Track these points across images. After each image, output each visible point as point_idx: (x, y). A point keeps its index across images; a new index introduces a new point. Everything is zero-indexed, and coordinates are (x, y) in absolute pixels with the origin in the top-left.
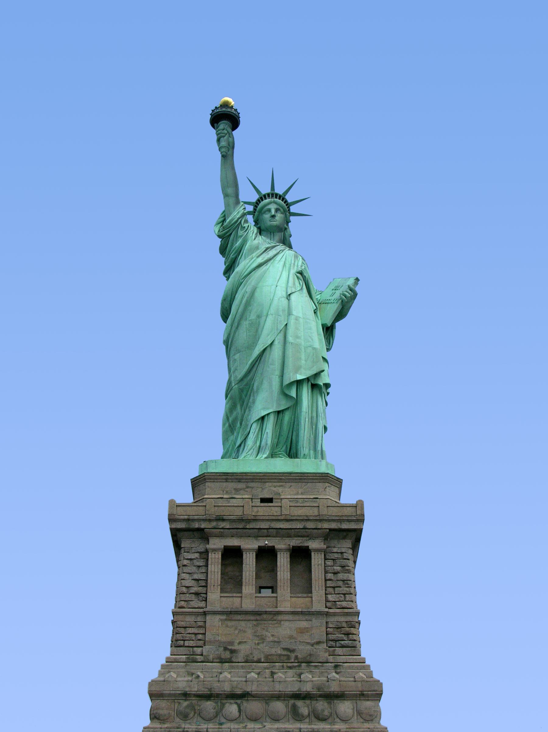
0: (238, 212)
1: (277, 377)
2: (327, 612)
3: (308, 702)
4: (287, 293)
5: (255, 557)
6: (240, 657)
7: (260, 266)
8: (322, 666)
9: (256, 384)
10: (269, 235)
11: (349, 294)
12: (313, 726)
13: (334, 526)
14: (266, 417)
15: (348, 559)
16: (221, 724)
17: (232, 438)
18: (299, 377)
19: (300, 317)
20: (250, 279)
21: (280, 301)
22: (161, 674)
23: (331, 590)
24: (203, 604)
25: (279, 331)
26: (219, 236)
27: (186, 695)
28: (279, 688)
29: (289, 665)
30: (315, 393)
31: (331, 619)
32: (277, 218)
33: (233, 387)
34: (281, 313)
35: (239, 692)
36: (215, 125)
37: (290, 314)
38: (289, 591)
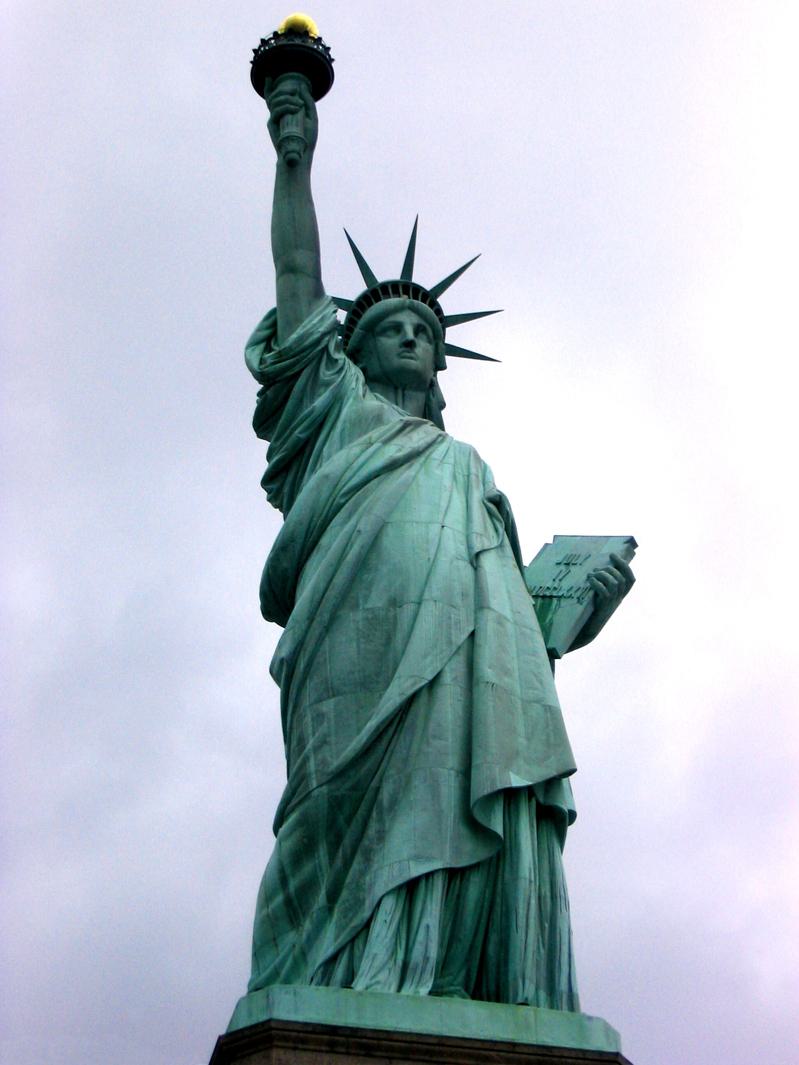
0: (322, 319)
1: (452, 772)
4: (469, 547)
7: (393, 466)
10: (392, 395)
11: (616, 578)
14: (423, 884)
17: (291, 938)
18: (517, 781)
19: (505, 618)
20: (366, 498)
21: (452, 568)
25: (454, 649)
26: (260, 376)
30: (545, 833)
32: (419, 351)
33: (313, 790)
34: (458, 601)
36: (268, 80)
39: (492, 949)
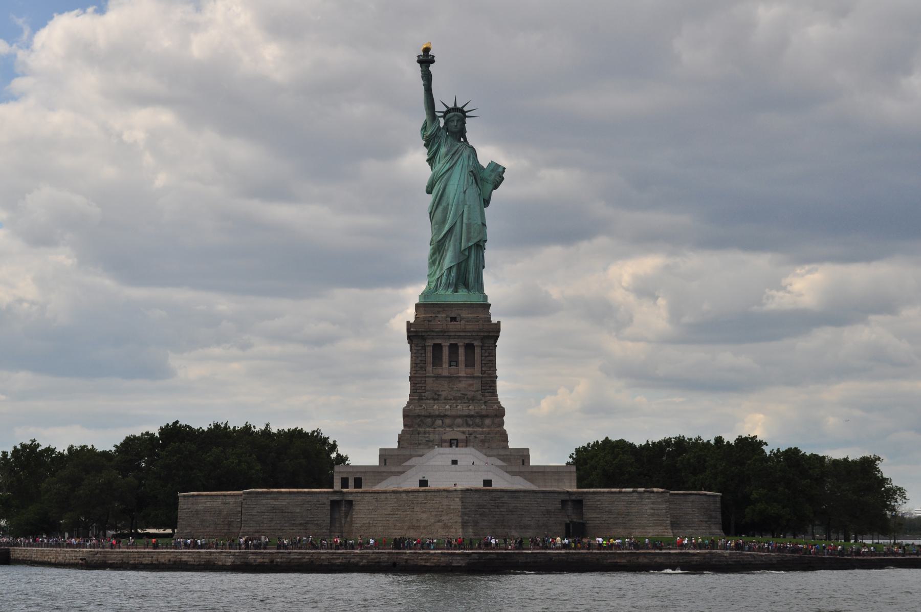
0: (435, 128)
3: (472, 418)
6: (442, 398)
9: (447, 246)
12: (475, 430)
13: (486, 334)
16: (435, 428)
18: (470, 244)
20: (442, 178)
22: (408, 406)
23: (483, 365)
24: (425, 372)
27: (419, 416)
28: (460, 413)
29: (464, 401)
35: (442, 414)
37: (464, 203)
39: (467, 275)
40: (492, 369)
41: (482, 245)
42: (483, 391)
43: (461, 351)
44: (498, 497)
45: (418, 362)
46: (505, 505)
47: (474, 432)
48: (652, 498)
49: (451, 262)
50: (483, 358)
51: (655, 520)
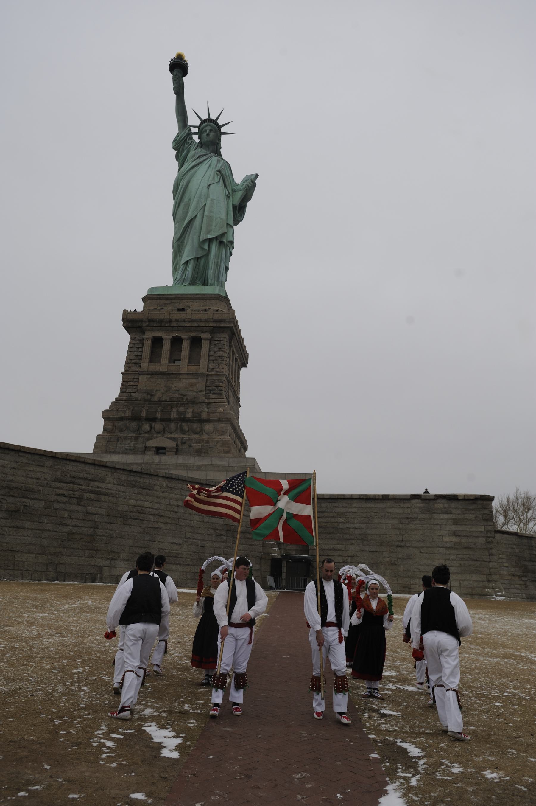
2: (208, 374)
3: (189, 423)
5: (170, 342)
7: (193, 167)
8: (201, 404)
15: (224, 344)
18: (210, 237)
19: (214, 200)
23: (211, 362)
24: (138, 369)
26: (175, 150)
31: (209, 378)
38: (187, 361)
40: (221, 366)
41: (225, 241)
42: (208, 391)
43: (186, 345)
44: (85, 476)
45: (132, 357)
46: (103, 498)
47: (189, 439)
48: (454, 511)
49: (188, 256)
50: (211, 354)
51: (462, 559)
